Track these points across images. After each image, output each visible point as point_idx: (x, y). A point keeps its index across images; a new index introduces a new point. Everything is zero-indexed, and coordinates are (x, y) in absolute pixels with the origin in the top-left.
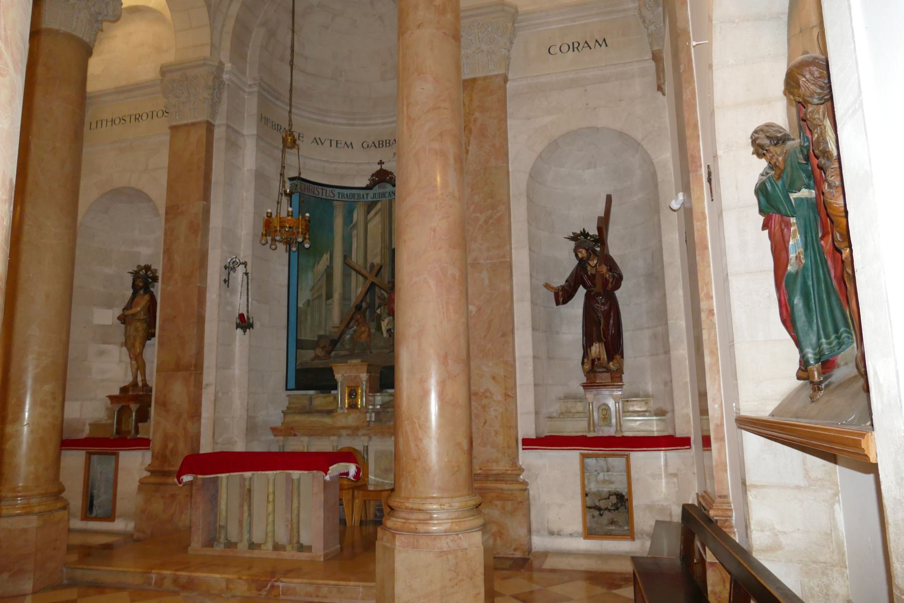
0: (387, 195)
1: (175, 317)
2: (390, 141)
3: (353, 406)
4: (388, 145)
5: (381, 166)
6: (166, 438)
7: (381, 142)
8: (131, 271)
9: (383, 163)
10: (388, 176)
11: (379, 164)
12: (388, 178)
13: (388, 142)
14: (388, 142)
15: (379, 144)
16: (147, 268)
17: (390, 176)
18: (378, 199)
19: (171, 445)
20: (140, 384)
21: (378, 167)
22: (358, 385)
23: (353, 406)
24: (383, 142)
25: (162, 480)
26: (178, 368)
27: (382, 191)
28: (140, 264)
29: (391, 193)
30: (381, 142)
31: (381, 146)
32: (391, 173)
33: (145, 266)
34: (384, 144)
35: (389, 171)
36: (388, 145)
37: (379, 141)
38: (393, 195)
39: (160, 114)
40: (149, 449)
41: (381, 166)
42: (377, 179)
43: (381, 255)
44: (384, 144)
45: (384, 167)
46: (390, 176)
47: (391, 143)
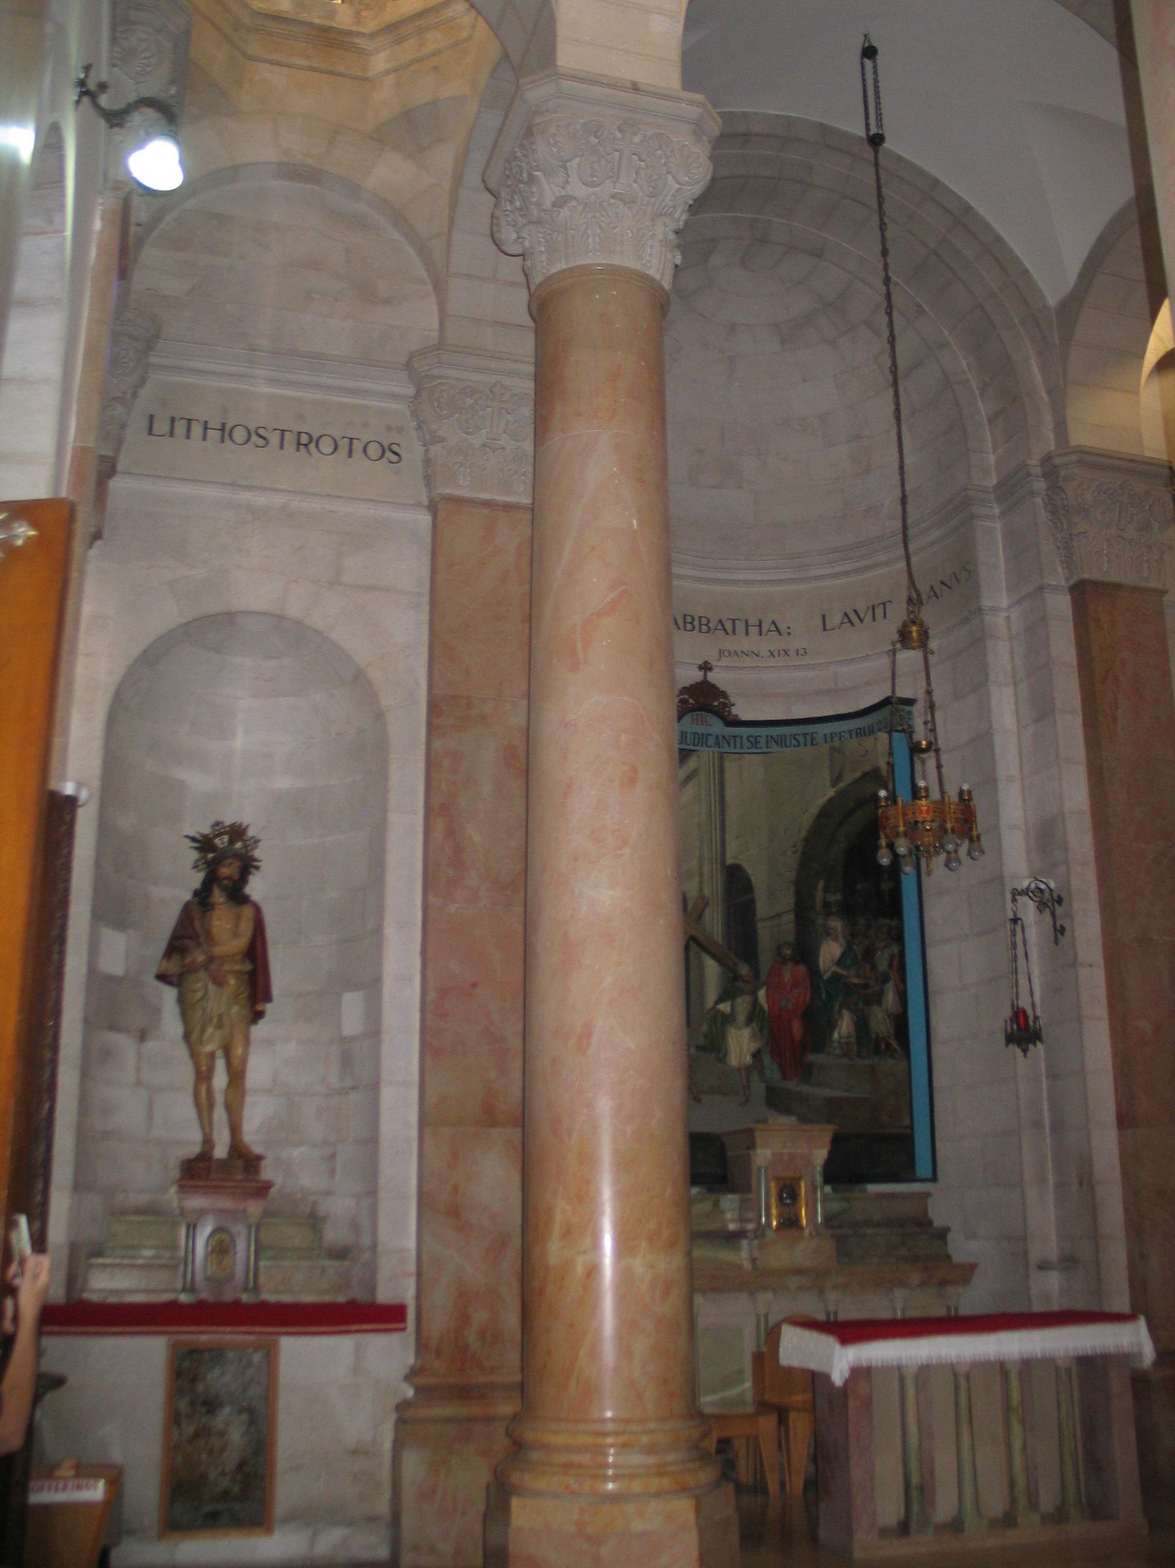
0: (711, 741)
1: (474, 985)
2: (709, 622)
3: (790, 1223)
4: (704, 628)
5: (705, 676)
6: (464, 1299)
7: (689, 619)
8: (192, 834)
9: (711, 669)
10: (717, 700)
11: (700, 668)
12: (716, 704)
13: (704, 621)
14: (704, 621)
15: (685, 622)
16: (237, 832)
17: (722, 700)
18: (693, 748)
19: (480, 1316)
20: (220, 1151)
21: (697, 676)
22: (798, 1175)
23: (790, 1223)
24: (693, 620)
25: (476, 1410)
26: (489, 1116)
27: (700, 729)
28: (220, 819)
29: (720, 738)
30: (689, 619)
31: (689, 626)
32: (724, 694)
33: (233, 826)
34: (696, 623)
35: (722, 688)
36: (704, 628)
37: (685, 616)
38: (726, 745)
39: (374, 450)
40: (404, 1329)
41: (705, 676)
42: (691, 701)
43: (701, 874)
44: (696, 623)
45: (712, 677)
46: (722, 700)
47: (712, 625)
